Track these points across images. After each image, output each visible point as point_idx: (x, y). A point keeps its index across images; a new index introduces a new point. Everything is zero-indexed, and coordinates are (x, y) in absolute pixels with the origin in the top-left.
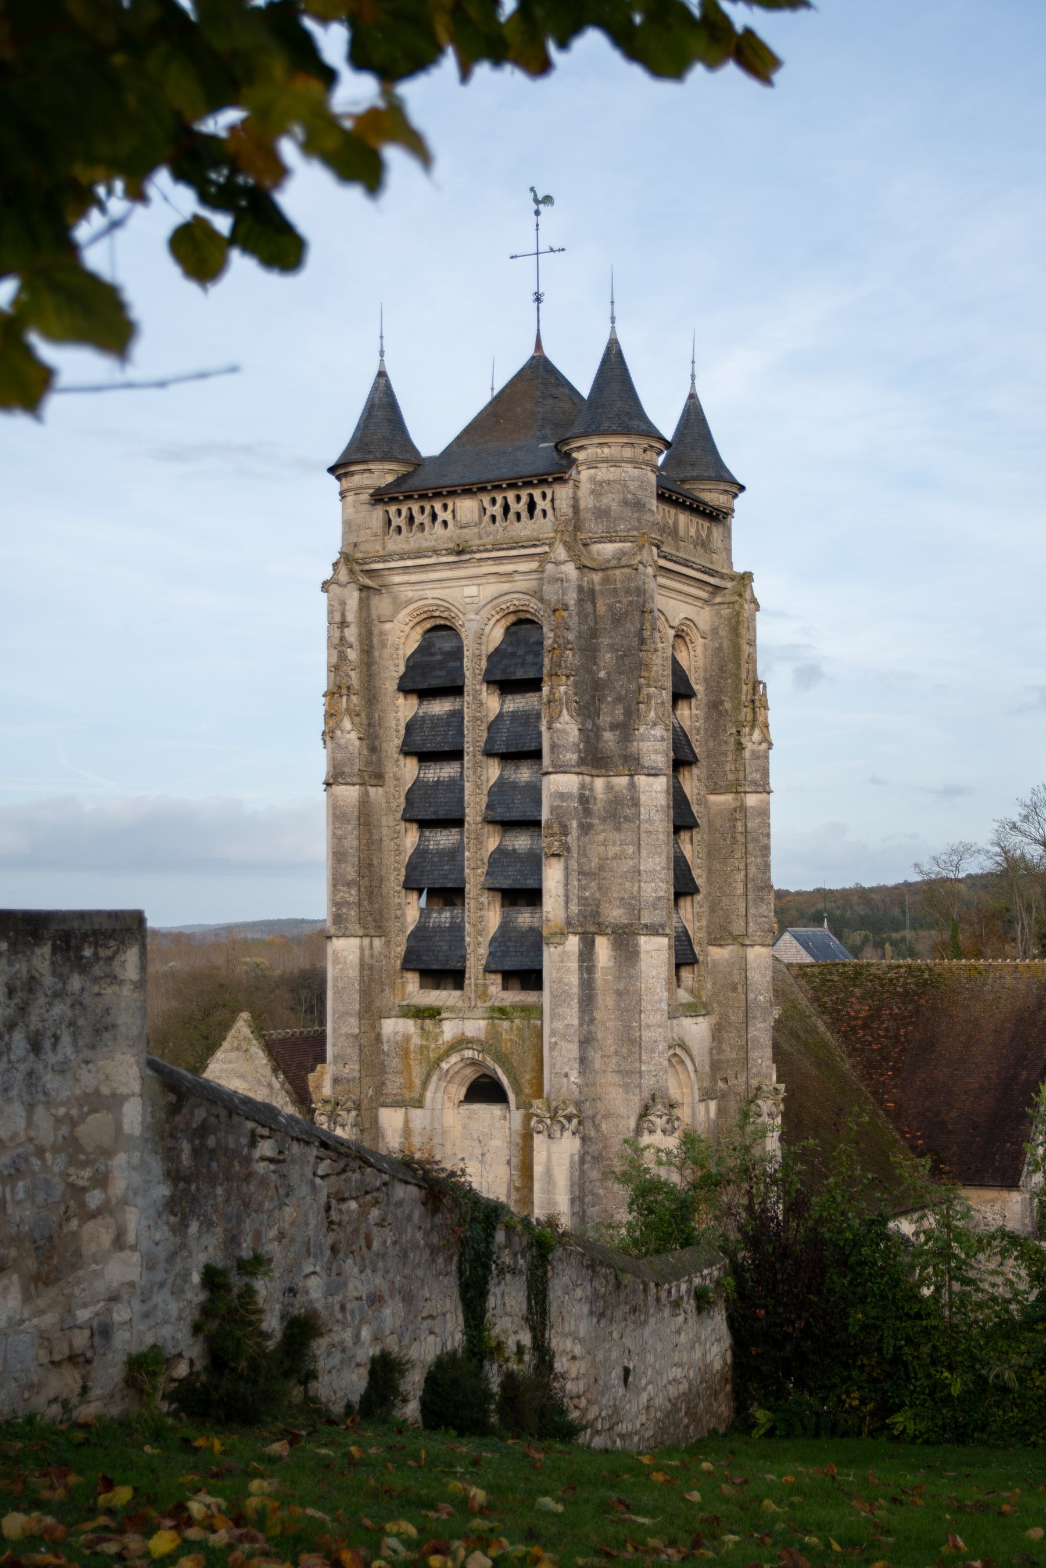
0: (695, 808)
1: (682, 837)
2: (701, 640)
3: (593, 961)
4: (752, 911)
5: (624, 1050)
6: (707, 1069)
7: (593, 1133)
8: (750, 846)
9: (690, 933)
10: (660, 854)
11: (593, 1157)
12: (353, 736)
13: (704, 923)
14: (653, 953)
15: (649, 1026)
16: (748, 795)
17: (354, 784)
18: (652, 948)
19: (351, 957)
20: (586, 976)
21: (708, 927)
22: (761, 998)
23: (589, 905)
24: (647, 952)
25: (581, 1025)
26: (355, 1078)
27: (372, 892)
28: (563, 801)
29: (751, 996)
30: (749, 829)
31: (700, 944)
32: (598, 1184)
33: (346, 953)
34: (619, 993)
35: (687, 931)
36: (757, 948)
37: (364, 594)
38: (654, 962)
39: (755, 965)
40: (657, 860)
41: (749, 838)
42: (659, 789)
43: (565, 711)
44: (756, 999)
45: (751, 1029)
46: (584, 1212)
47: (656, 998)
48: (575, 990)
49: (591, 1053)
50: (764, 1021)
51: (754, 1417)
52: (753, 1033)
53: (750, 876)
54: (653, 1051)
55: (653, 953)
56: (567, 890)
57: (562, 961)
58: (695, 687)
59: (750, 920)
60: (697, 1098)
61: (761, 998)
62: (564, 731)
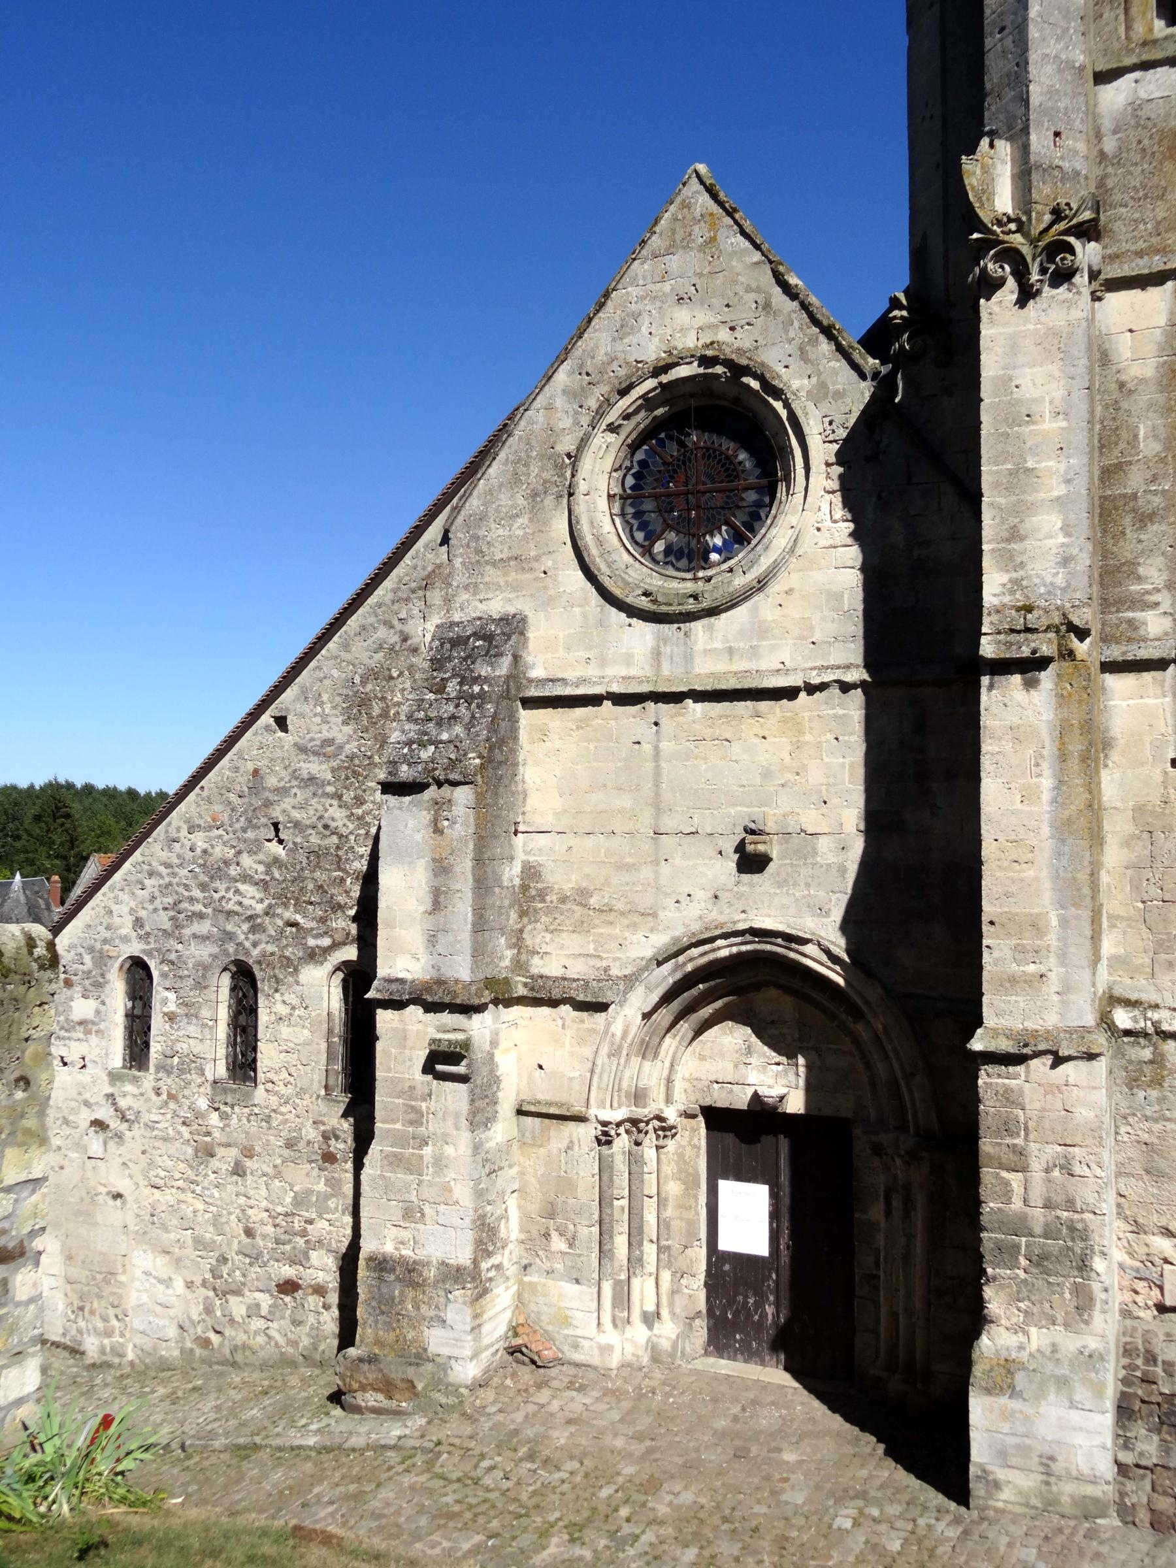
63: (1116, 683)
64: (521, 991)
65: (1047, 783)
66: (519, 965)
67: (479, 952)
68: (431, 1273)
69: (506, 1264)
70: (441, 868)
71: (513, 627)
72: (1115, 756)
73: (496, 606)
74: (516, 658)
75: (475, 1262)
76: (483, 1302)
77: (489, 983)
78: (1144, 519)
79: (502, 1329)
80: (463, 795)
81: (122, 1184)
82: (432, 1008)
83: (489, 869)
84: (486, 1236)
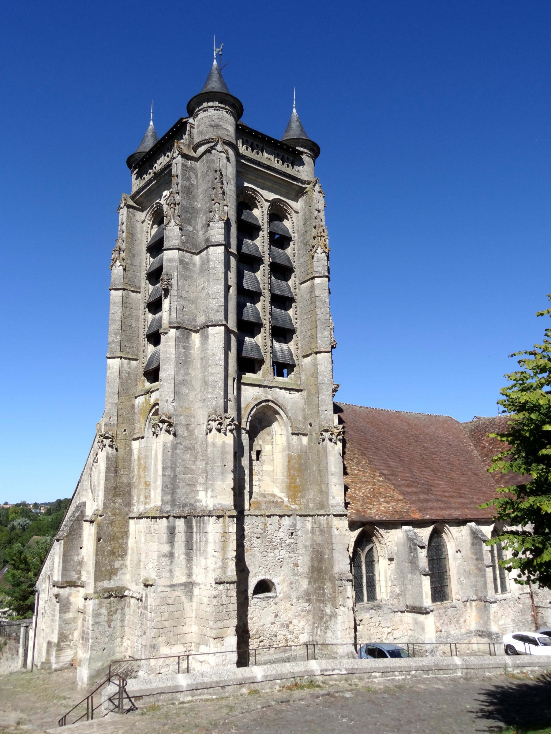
1: (287, 305)
4: (319, 335)
5: (203, 388)
6: (300, 418)
7: (186, 433)
8: (318, 303)
9: (292, 351)
10: (220, 284)
11: (185, 447)
14: (216, 335)
15: (213, 374)
18: (215, 332)
19: (115, 367)
20: (182, 350)
21: (301, 347)
22: (326, 379)
23: (186, 315)
24: (213, 335)
25: (176, 374)
26: (114, 424)
27: (131, 339)
29: (320, 378)
31: (297, 356)
32: (191, 463)
33: (113, 365)
34: (202, 359)
38: (216, 339)
39: (322, 362)
42: (220, 252)
43: (172, 221)
44: (322, 380)
45: (320, 395)
46: (175, 476)
47: (217, 358)
48: (173, 356)
49: (185, 390)
50: (328, 391)
51: (326, 611)
52: (321, 397)
53: (318, 318)
54: (215, 387)
55: (216, 335)
56: (170, 306)
57: (166, 342)
58: (292, 235)
59: (319, 339)
61: (326, 379)
62: (173, 230)
63: (131, 521)
64: (79, 584)
65: (93, 545)
66: (79, 578)
67: (63, 575)
68: (53, 644)
69: (71, 645)
70: (60, 558)
71: (84, 504)
72: (130, 537)
73: (83, 500)
74: (82, 512)
75: (58, 642)
76: (61, 652)
77: (67, 582)
78: (135, 487)
79: (69, 659)
80: (62, 542)
81: (44, 628)
82: (57, 587)
83: (69, 558)
84: (63, 637)
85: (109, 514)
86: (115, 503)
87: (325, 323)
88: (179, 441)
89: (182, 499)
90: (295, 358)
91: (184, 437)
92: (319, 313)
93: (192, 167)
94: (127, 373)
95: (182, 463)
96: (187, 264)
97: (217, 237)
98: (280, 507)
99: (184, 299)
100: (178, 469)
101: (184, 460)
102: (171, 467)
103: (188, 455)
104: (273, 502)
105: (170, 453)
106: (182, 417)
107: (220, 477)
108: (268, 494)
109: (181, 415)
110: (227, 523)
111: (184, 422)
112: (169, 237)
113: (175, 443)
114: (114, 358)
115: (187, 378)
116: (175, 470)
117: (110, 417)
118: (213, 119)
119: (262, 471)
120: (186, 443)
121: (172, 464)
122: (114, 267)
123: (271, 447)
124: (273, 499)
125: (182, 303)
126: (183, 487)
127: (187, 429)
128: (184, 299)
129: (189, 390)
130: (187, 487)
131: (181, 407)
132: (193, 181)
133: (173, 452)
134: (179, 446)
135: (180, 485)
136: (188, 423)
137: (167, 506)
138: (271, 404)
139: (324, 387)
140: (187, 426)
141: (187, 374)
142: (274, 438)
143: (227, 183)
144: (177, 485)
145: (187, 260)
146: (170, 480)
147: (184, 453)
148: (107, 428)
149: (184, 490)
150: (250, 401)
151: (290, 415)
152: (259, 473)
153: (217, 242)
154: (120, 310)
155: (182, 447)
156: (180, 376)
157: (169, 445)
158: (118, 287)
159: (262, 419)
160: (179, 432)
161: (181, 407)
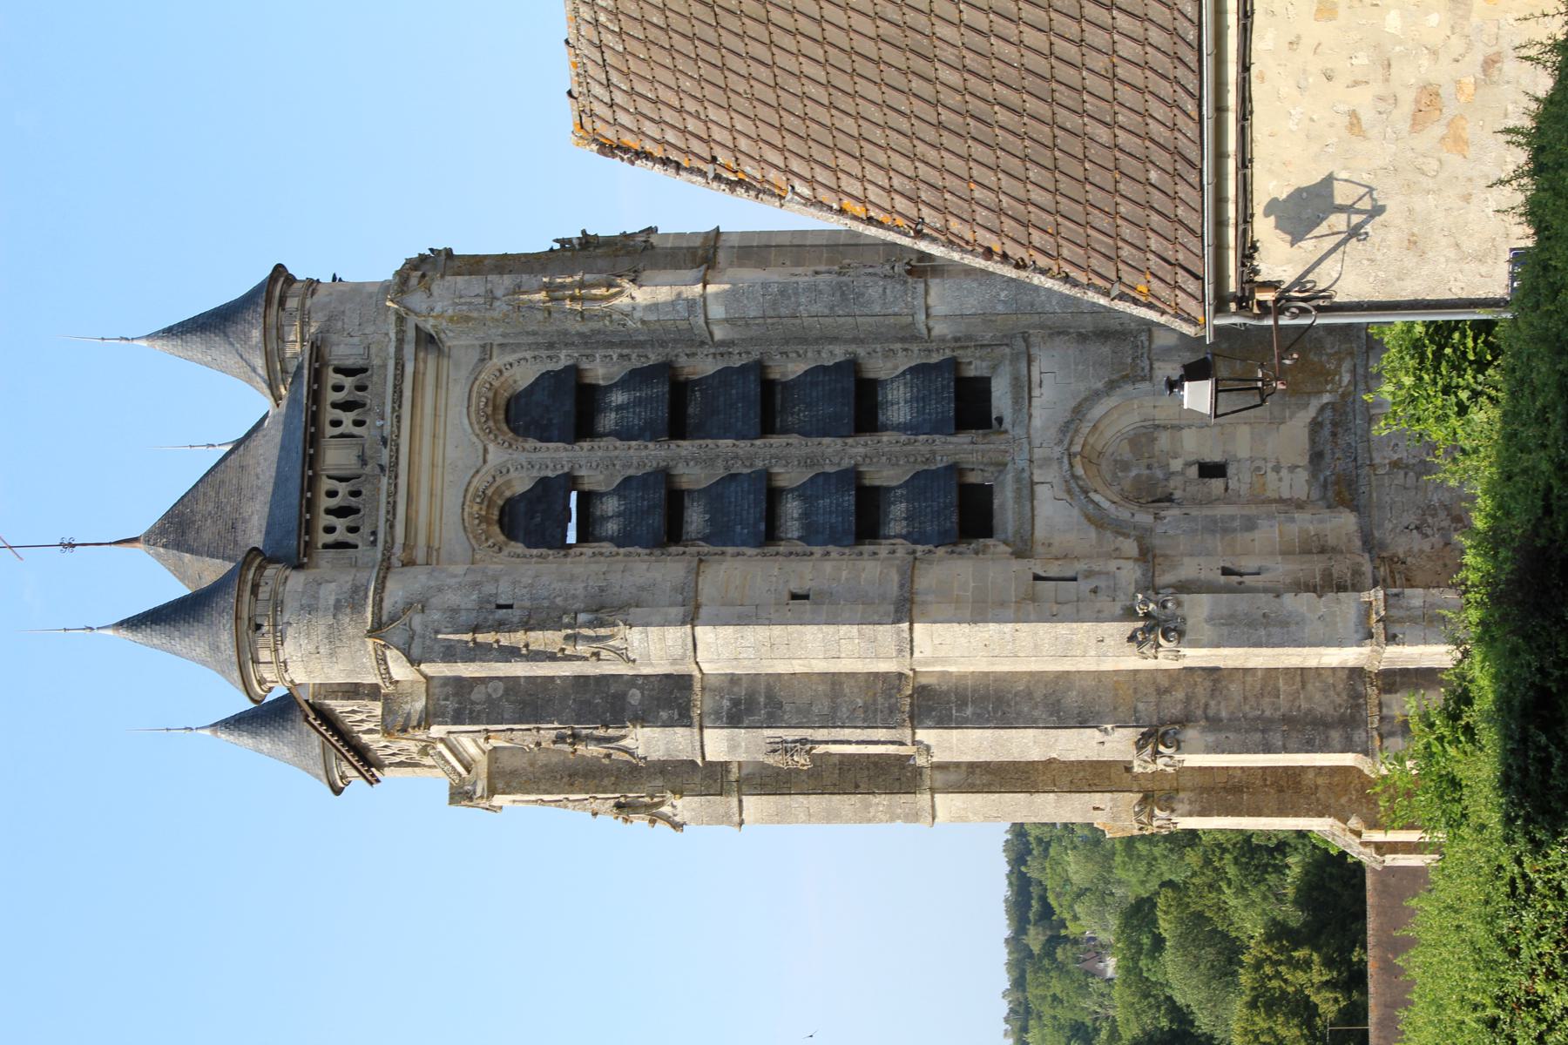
0: (737, 362)
2: (495, 360)
3: (947, 693)
4: (877, 309)
6: (1106, 350)
7: (1180, 695)
11: (1212, 696)
12: (679, 802)
13: (898, 346)
16: (711, 316)
17: (740, 801)
20: (969, 711)
22: (1003, 294)
23: (875, 701)
28: (739, 745)
29: (1000, 308)
30: (760, 314)
35: (911, 370)
36: (930, 301)
37: (500, 785)
40: (809, 637)
41: (770, 313)
45: (1048, 308)
48: (988, 732)
53: (827, 312)
54: (1069, 642)
57: (951, 749)
60: (1145, 386)
61: (1003, 294)
85: (1344, 800)
86: (1317, 787)
87: (843, 294)
88: (1199, 712)
89: (1338, 701)
90: (935, 358)
91: (1188, 699)
92: (814, 309)
93: (455, 695)
94: (973, 773)
95: (1253, 702)
96: (736, 703)
97: (670, 643)
98: (1346, 413)
99: (834, 709)
100: (1268, 713)
101: (1245, 698)
102: (1263, 731)
103: (1233, 687)
104: (1334, 434)
105: (1232, 736)
106: (1141, 706)
107: (1293, 628)
108: (1313, 441)
109: (1136, 711)
110: (1402, 613)
111: (1153, 699)
112: (668, 749)
113: (1203, 723)
114: (933, 807)
115: (1039, 695)
116: (1271, 721)
117: (1096, 809)
118: (311, 648)
119: (1252, 459)
120: (1201, 692)
121: (1257, 730)
122: (677, 819)
123: (1186, 432)
124: (1326, 431)
125: (844, 712)
126: (1309, 699)
127: (1167, 691)
128: (834, 709)
129: (1069, 689)
130: (1309, 687)
131: (1115, 709)
132: (495, 690)
133: (1227, 728)
134: (1211, 713)
135: (1305, 706)
136: (1151, 690)
137: (1356, 738)
138: (1076, 448)
139: (1026, 298)
140: (1161, 692)
141: (1029, 694)
142: (1162, 423)
143: (499, 607)
144: (1306, 714)
145: (726, 703)
146: (1294, 734)
147: (1226, 698)
148: (1124, 816)
149: (1318, 696)
150: (1076, 512)
151: (1100, 385)
152: (1258, 469)
153: (684, 645)
154: (800, 798)
155: (1213, 703)
156: (1036, 713)
157: (1210, 738)
158: (736, 809)
159: (1116, 461)
160: (1177, 711)
161: (1115, 709)
